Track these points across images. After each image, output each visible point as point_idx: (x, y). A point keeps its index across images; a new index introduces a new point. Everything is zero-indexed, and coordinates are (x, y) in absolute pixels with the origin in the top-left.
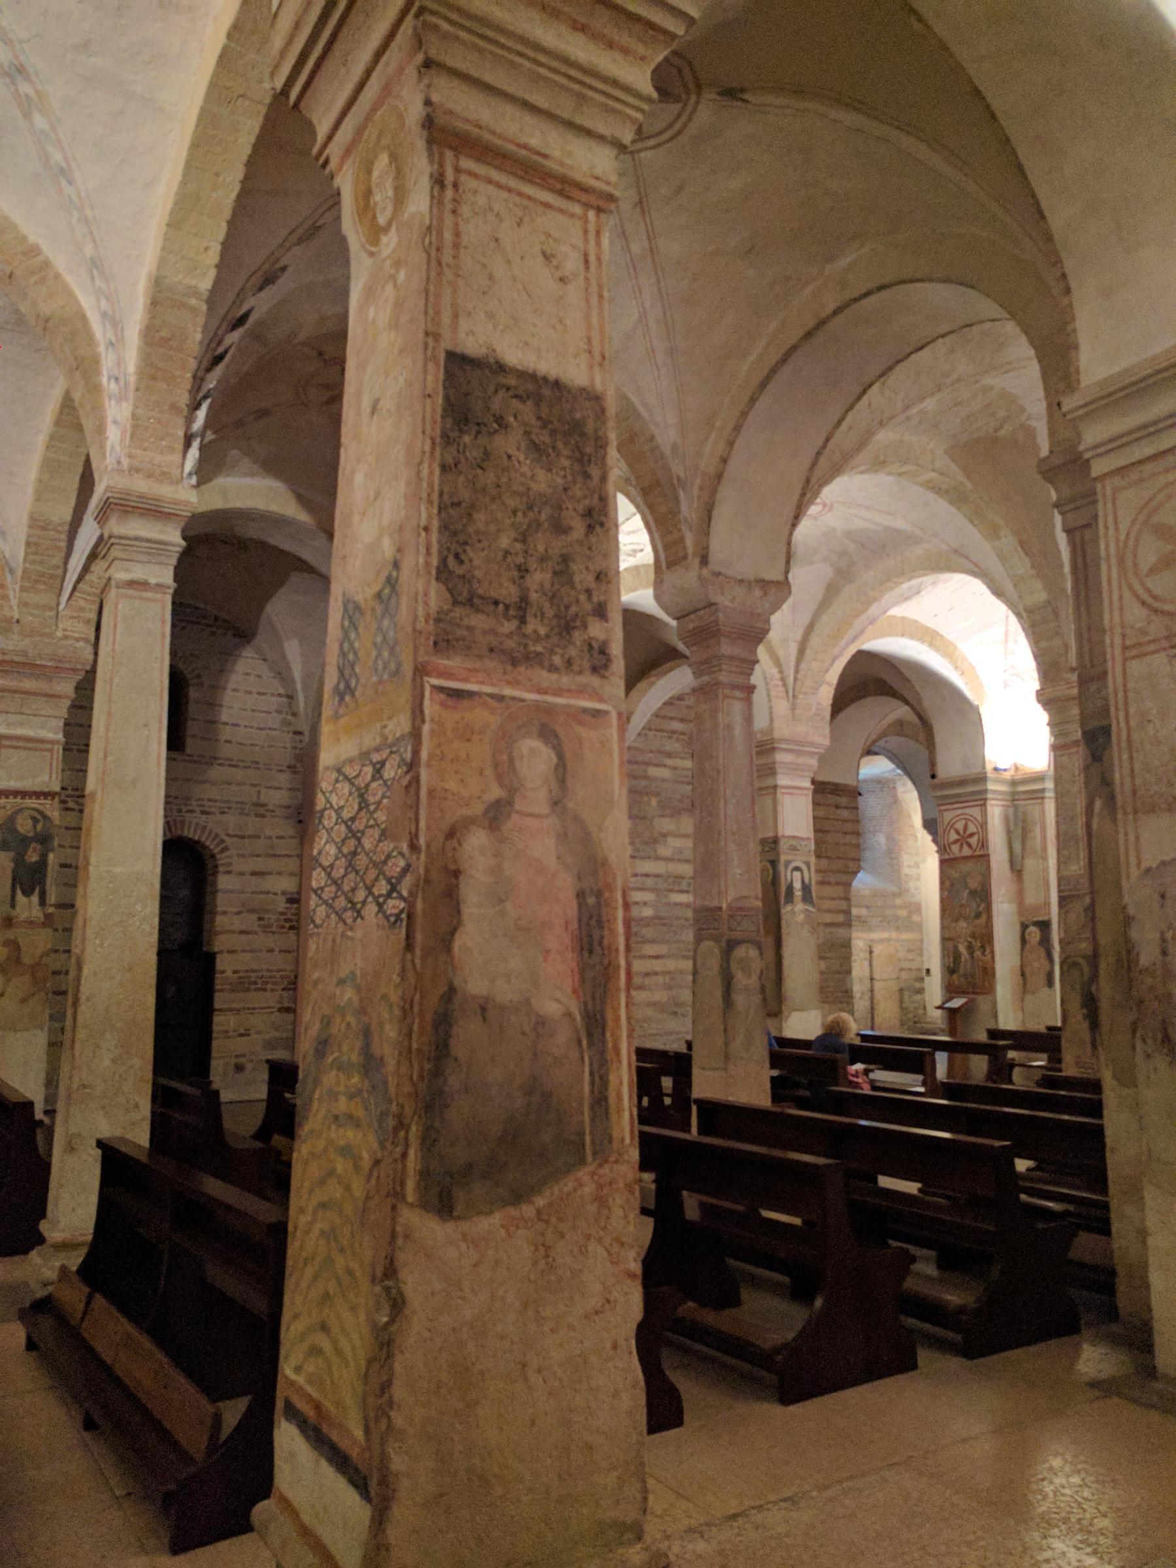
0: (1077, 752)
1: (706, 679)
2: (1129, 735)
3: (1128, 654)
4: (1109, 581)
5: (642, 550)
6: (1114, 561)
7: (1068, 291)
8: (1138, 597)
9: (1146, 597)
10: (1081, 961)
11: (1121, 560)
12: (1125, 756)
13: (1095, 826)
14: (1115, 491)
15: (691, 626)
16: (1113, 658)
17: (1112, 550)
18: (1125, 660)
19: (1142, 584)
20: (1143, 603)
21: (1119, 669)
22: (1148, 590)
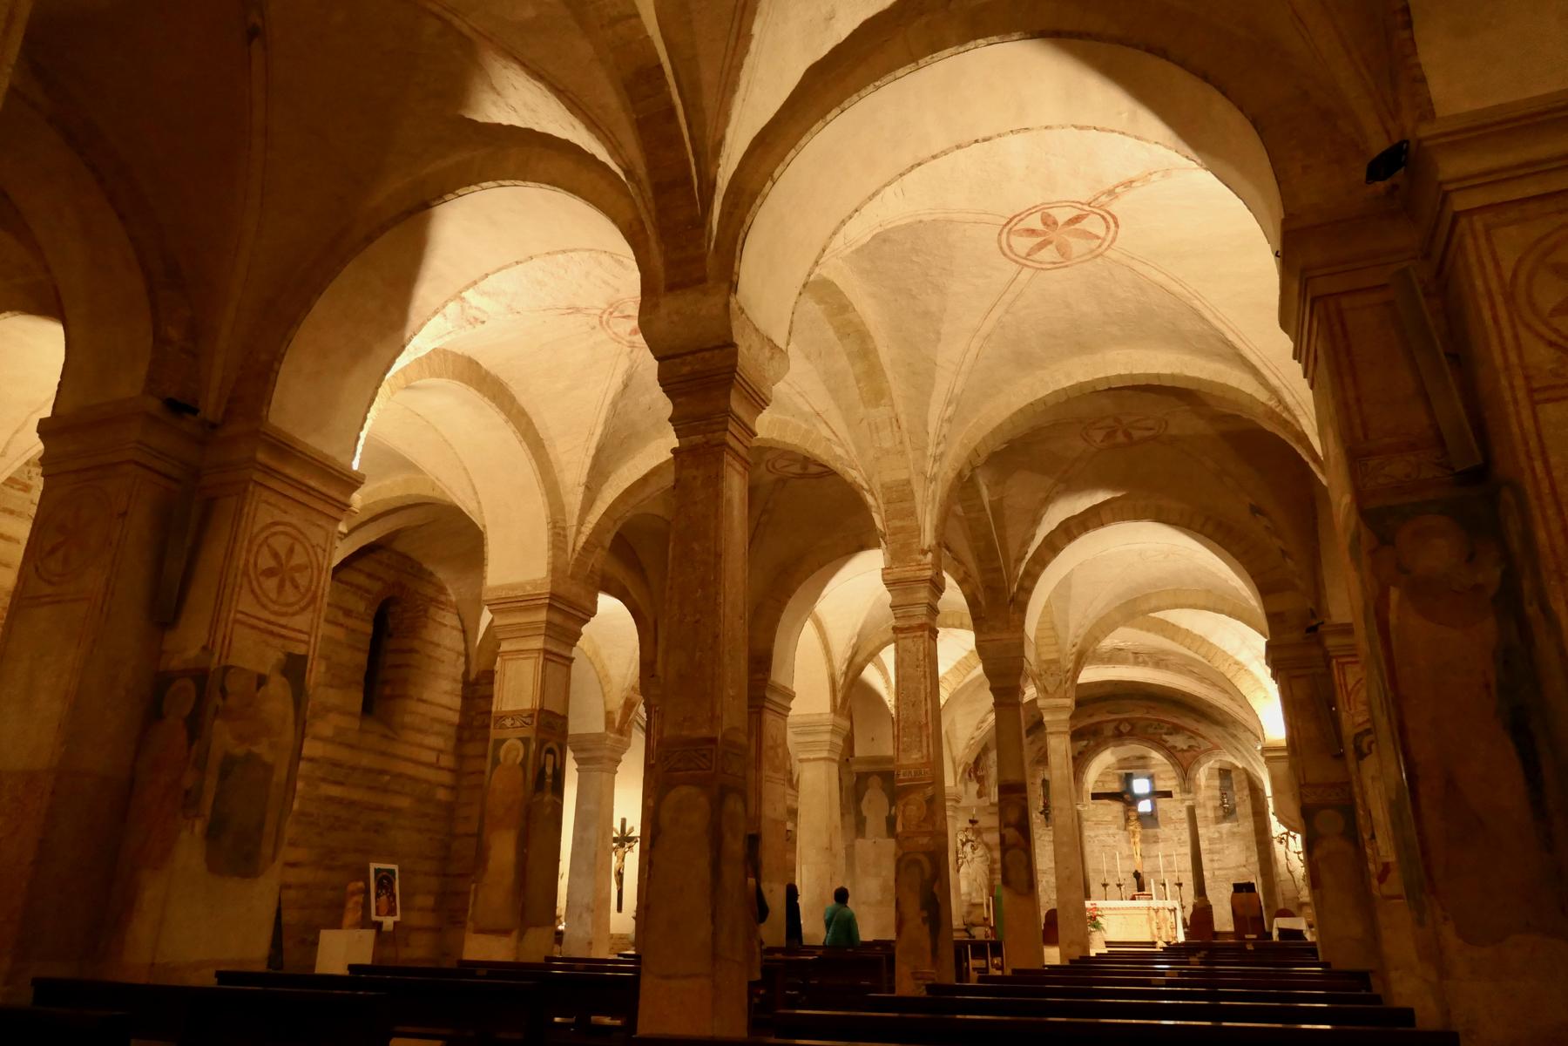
0: (921, 636)
1: (697, 439)
2: (1553, 487)
3: (1537, 397)
4: (1495, 319)
5: (483, 322)
6: (1499, 299)
7: (1409, 25)
8: (1541, 337)
9: (1554, 337)
10: (922, 858)
11: (1510, 298)
12: (1551, 512)
13: (1393, 618)
14: (1488, 230)
15: (686, 370)
16: (1516, 402)
17: (1494, 285)
18: (1534, 404)
19: (1547, 324)
20: (1551, 344)
21: (1526, 414)
22: (1556, 331)
